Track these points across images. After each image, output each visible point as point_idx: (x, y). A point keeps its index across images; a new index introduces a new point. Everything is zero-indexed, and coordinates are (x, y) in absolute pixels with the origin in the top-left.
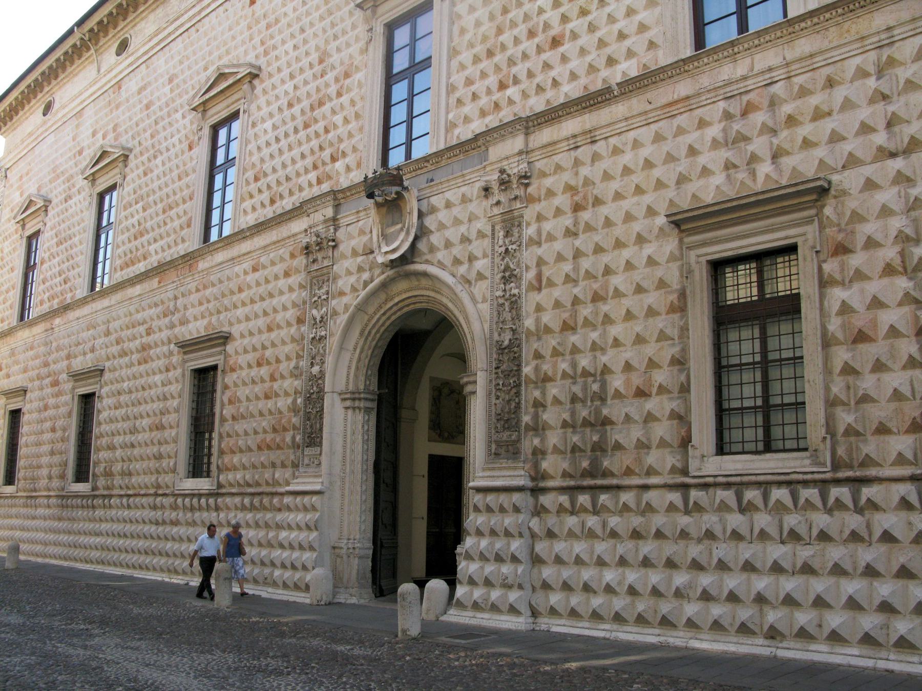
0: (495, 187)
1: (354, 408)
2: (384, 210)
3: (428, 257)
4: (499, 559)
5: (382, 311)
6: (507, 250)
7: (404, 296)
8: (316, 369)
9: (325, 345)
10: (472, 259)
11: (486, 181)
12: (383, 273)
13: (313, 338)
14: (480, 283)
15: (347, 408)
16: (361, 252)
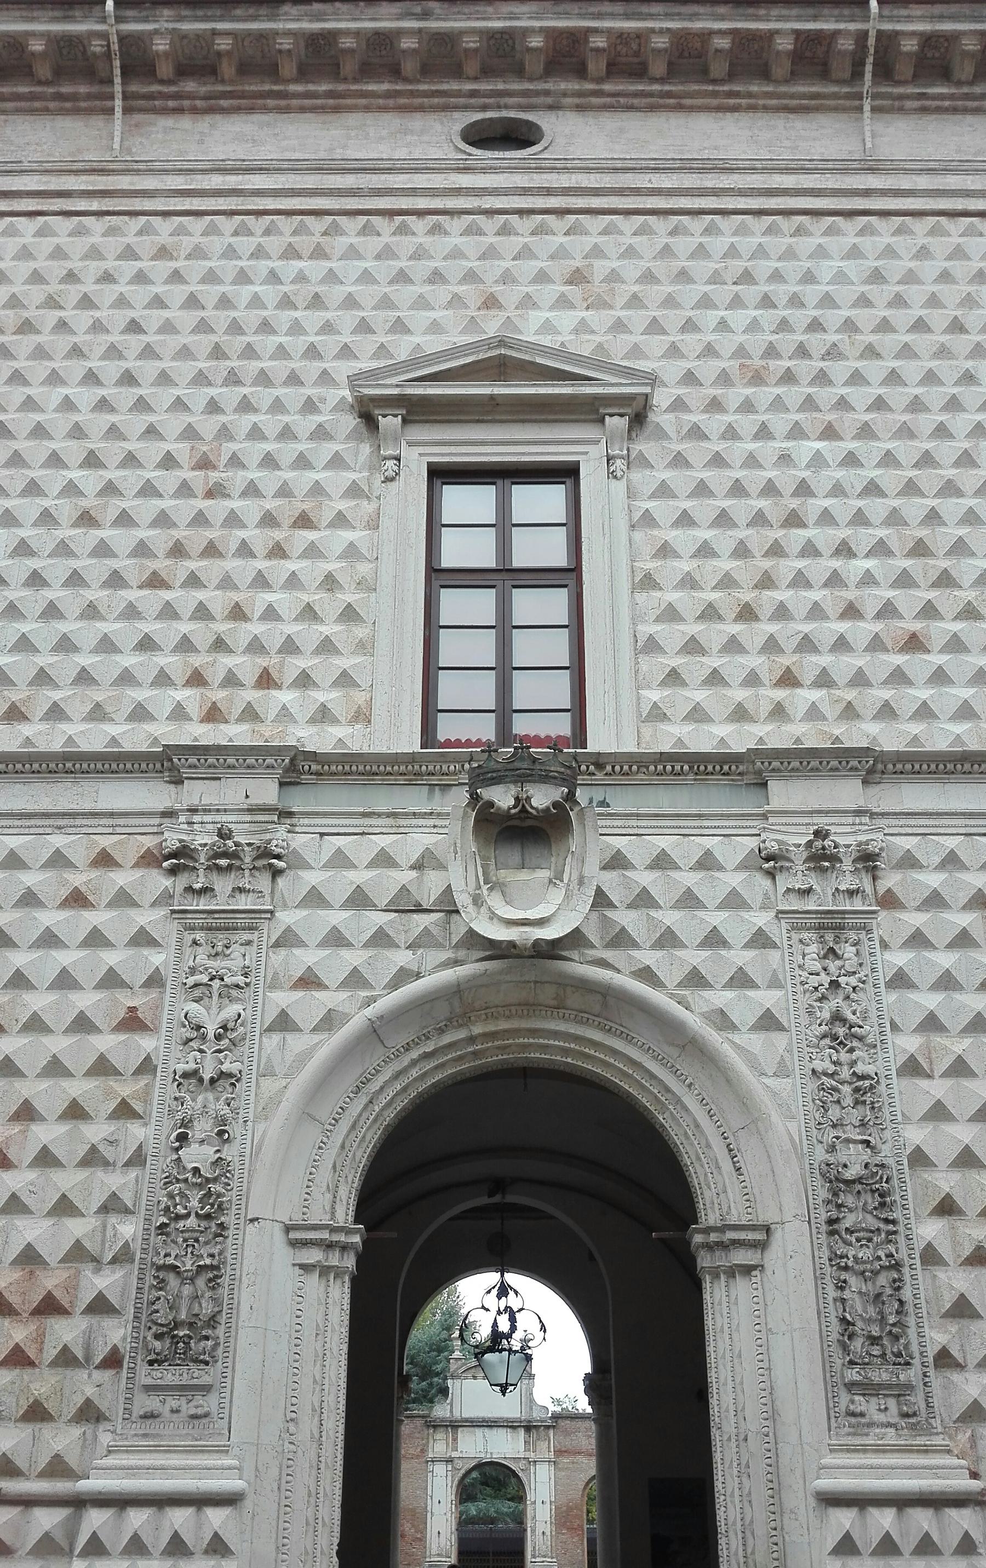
0: (799, 857)
1: (325, 1271)
3: (608, 955)
5: (429, 1047)
6: (835, 985)
8: (197, 1155)
12: (456, 962)
13: (192, 1075)
15: (306, 1268)
16: (383, 902)
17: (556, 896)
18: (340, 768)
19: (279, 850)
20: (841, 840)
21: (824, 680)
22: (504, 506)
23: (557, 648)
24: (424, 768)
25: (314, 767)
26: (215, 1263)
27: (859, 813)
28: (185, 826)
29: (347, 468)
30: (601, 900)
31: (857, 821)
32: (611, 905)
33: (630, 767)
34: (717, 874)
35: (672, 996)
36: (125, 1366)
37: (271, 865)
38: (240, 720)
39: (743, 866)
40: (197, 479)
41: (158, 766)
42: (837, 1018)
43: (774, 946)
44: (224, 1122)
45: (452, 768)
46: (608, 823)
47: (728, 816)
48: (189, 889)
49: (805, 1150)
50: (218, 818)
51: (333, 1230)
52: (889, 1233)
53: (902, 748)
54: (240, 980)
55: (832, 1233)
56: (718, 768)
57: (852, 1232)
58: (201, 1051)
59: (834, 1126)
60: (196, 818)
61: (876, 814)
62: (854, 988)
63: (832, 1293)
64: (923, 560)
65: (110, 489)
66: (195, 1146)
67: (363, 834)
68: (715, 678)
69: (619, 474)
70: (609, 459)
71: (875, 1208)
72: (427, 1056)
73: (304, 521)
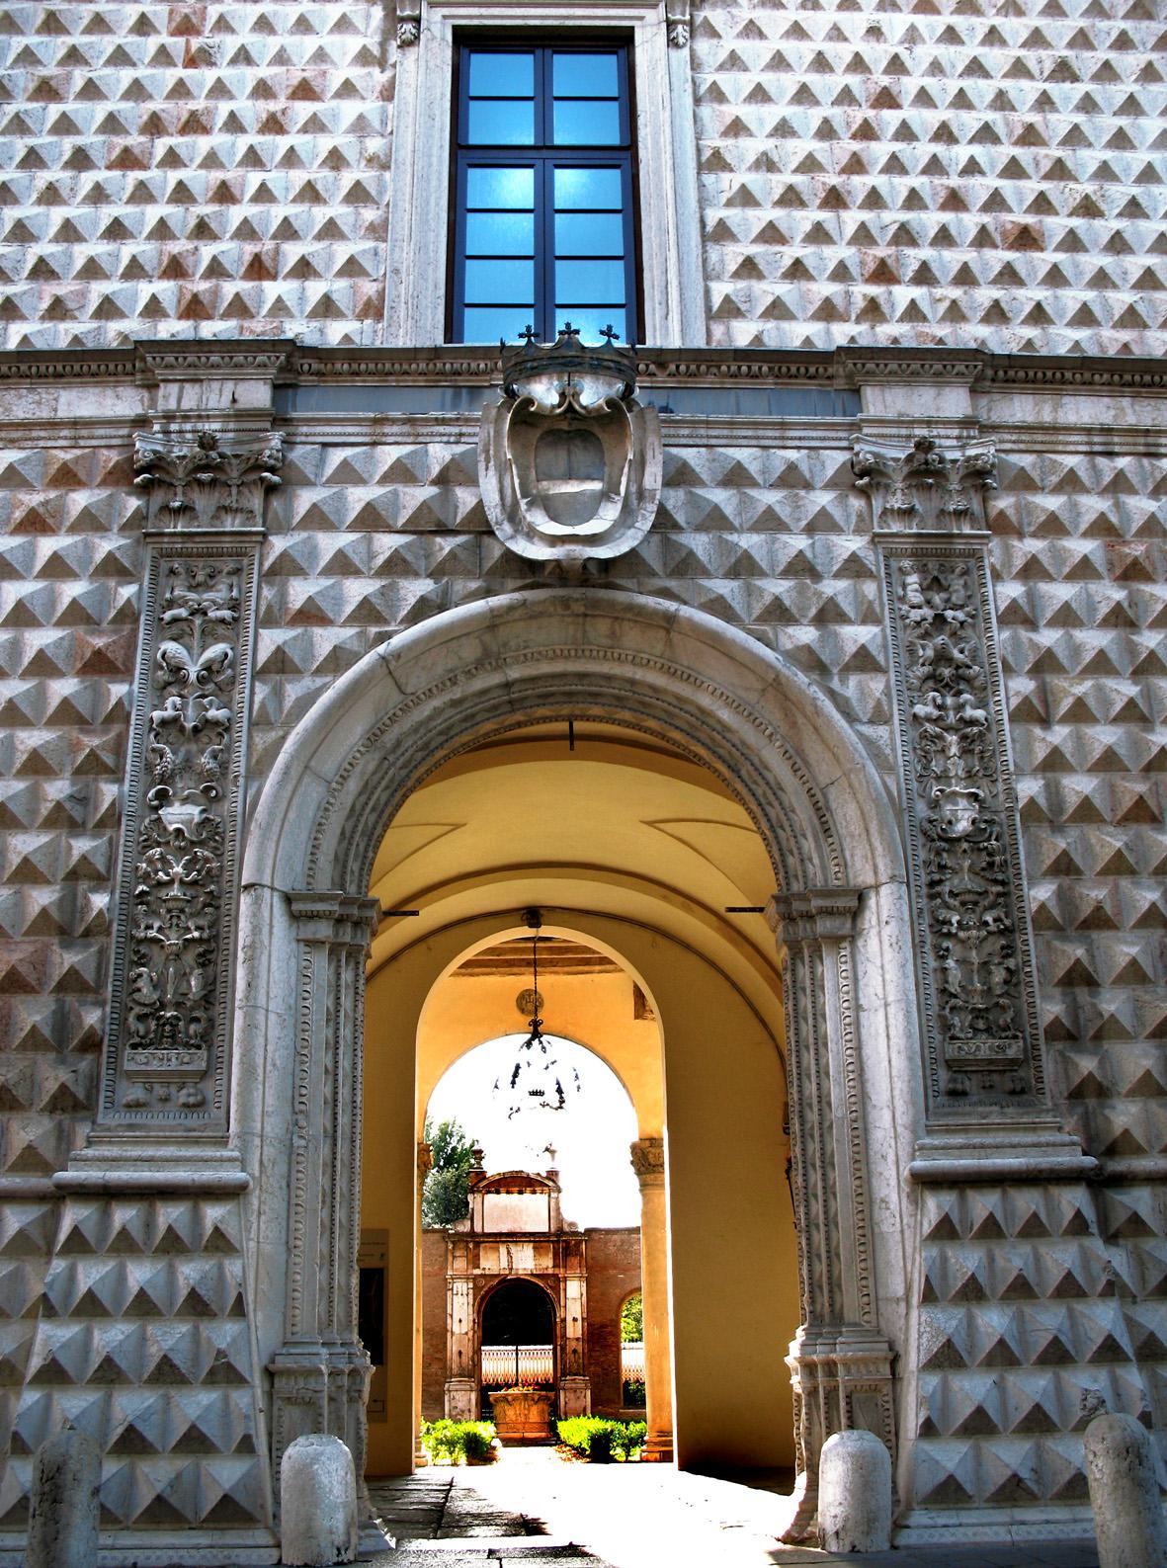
1: (335, 950)
2: (535, 435)
3: (672, 584)
4: (1057, 1355)
6: (940, 620)
7: (546, 668)
9: (228, 749)
10: (828, 615)
11: (876, 455)
12: (488, 592)
14: (853, 680)
17: (610, 513)
18: (346, 366)
19: (272, 462)
20: (950, 455)
21: (924, 276)
22: (543, 78)
23: (609, 234)
24: (448, 366)
25: (315, 366)
26: (205, 935)
27: (966, 423)
28: (160, 436)
29: (356, 31)
30: (664, 522)
31: (965, 434)
32: (676, 527)
33: (698, 367)
34: (802, 493)
35: (750, 632)
36: (105, 1049)
37: (262, 479)
38: (227, 315)
39: (831, 485)
40: (177, 44)
41: (129, 367)
42: (942, 657)
43: (871, 575)
44: (210, 775)
45: (482, 366)
46: (672, 431)
47: (814, 426)
48: (165, 509)
49: (905, 805)
50: (200, 426)
51: (345, 902)
52: (999, 895)
53: (1015, 352)
54: (226, 614)
55: (932, 897)
56: (802, 370)
57: (957, 895)
58: (180, 696)
59: (938, 778)
60: (174, 427)
61: (985, 426)
62: (962, 623)
63: (933, 963)
64: (1033, 149)
65: (74, 56)
66: (177, 804)
67: (374, 444)
68: (797, 271)
69: (681, 40)
70: (671, 25)
71: (983, 869)
72: (455, 703)
73: (305, 91)
